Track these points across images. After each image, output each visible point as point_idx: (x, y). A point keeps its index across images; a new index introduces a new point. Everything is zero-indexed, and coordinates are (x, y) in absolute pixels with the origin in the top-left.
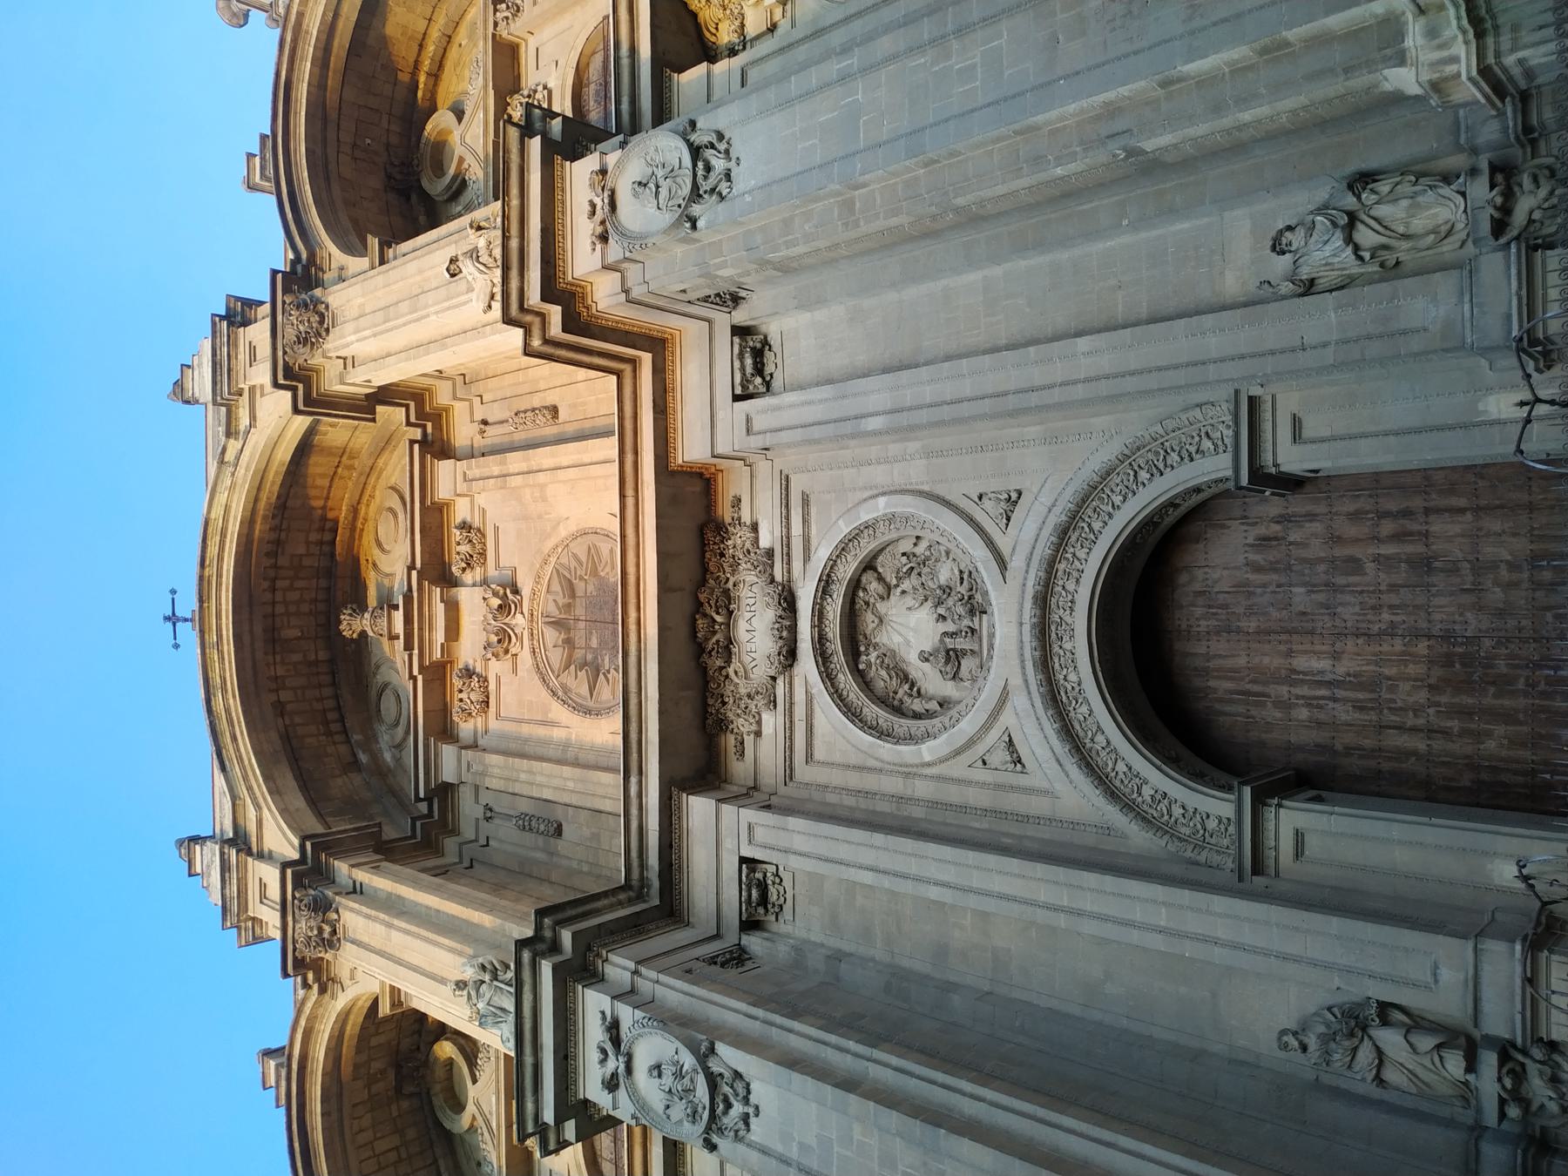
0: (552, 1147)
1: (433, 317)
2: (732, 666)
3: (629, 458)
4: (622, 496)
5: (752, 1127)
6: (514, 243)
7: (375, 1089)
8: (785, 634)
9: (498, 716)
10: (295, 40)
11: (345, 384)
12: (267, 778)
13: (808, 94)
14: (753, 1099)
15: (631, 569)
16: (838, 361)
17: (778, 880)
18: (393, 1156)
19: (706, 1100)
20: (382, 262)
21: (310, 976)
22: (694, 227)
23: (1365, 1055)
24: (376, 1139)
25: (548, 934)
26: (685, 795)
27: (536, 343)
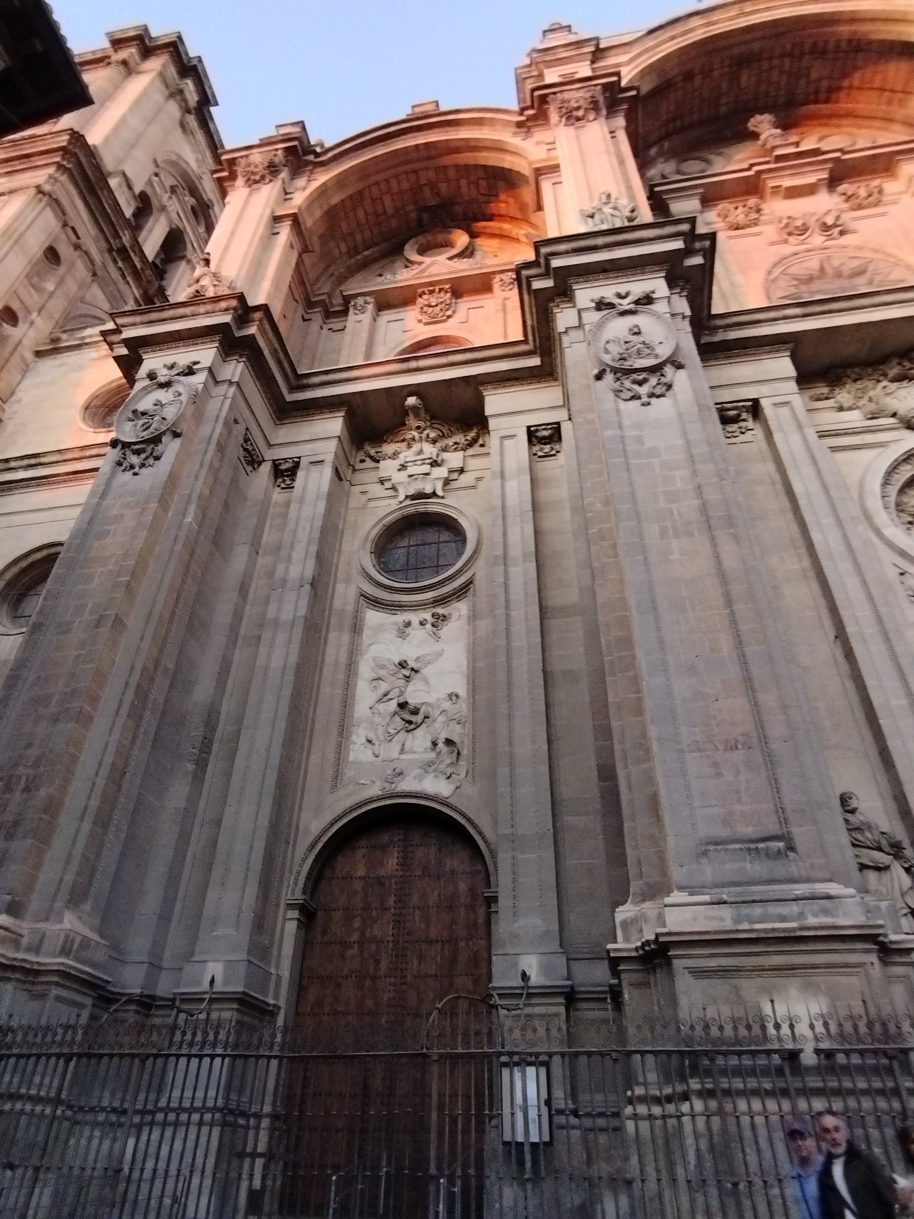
0: (525, 273)
5: (630, 402)
7: (427, 190)
9: (730, 237)
12: (650, 66)
14: (654, 401)
17: (743, 430)
18: (380, 209)
19: (637, 366)
21: (531, 112)
23: (881, 858)
24: (392, 194)
25: (697, 245)
26: (788, 354)
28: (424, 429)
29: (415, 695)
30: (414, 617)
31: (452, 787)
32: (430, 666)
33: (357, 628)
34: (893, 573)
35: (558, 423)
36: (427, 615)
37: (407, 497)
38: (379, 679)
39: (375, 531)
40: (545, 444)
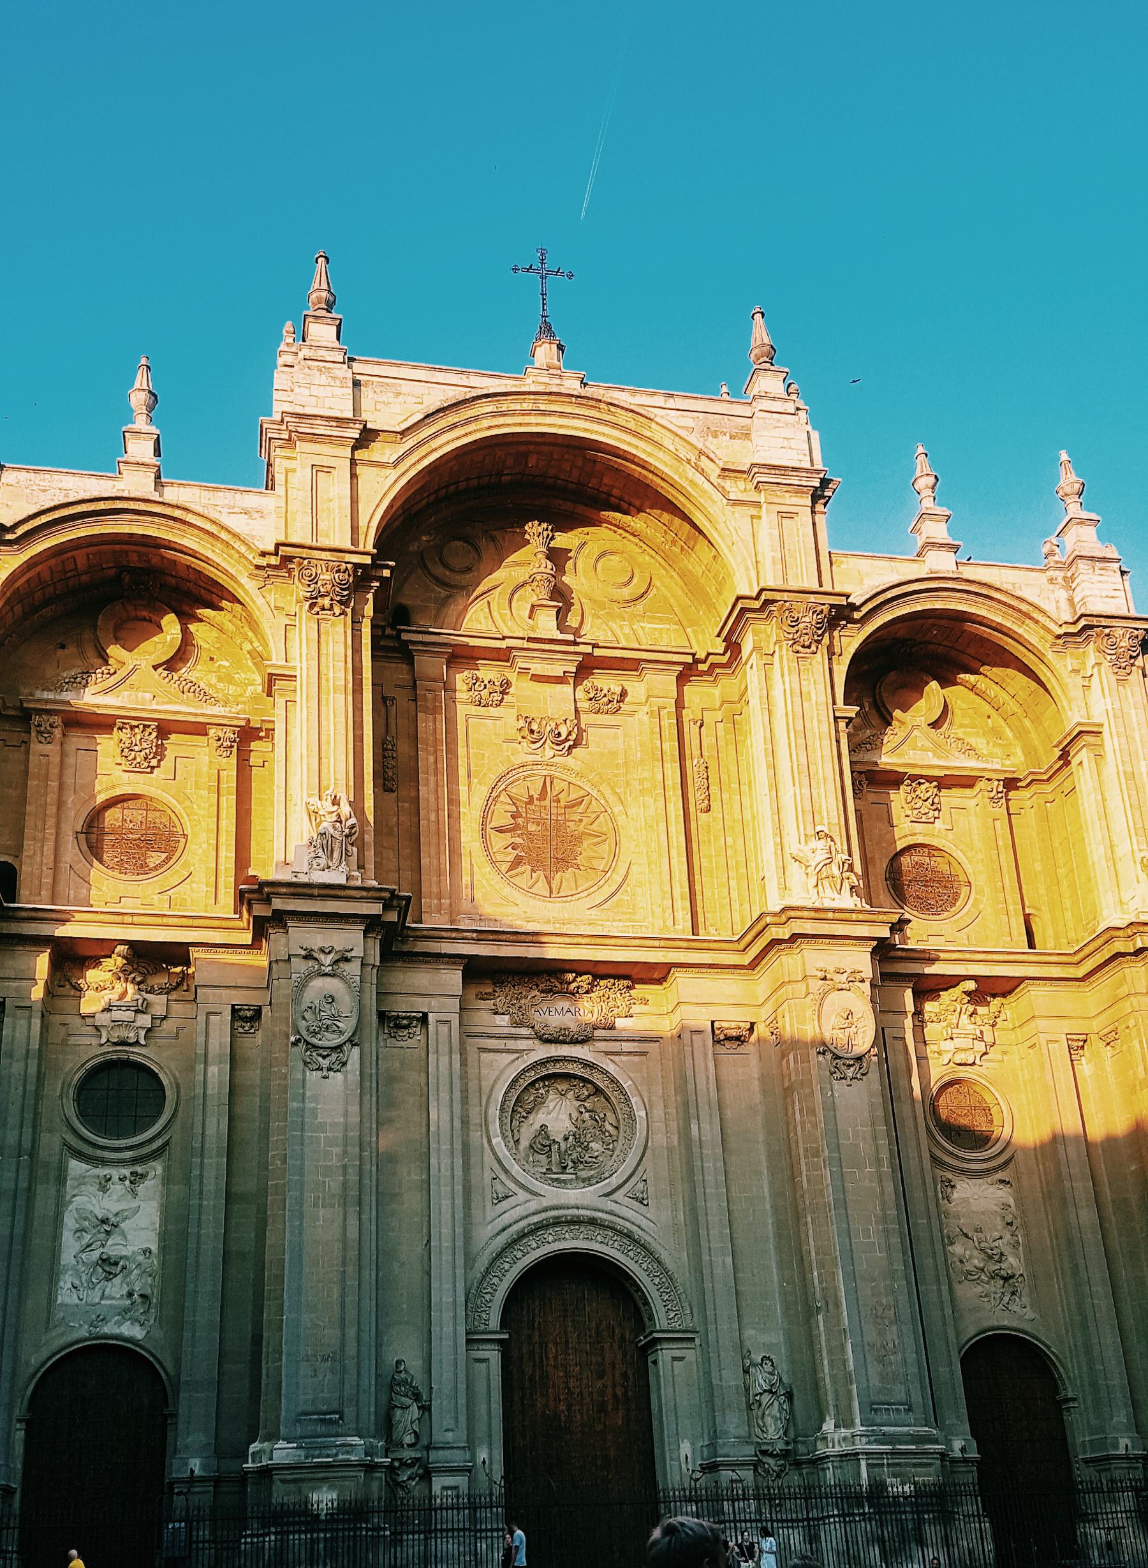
1: (792, 789)
2: (539, 994)
3: (684, 944)
4: (661, 939)
5: (314, 1073)
6: (830, 915)
8: (561, 1038)
10: (1019, 611)
11: (754, 649)
13: (875, 1138)
14: (331, 1073)
15: (613, 941)
16: (728, 1096)
20: (836, 718)
22: (819, 1053)
25: (395, 903)
27: (768, 919)
28: (131, 973)
29: (114, 1247)
30: (115, 1173)
31: (144, 1332)
32: (127, 1221)
33: (61, 1180)
34: (488, 1176)
35: (260, 1006)
36: (126, 1172)
37: (108, 1041)
38: (83, 1230)
39: (77, 1076)
40: (247, 1022)
